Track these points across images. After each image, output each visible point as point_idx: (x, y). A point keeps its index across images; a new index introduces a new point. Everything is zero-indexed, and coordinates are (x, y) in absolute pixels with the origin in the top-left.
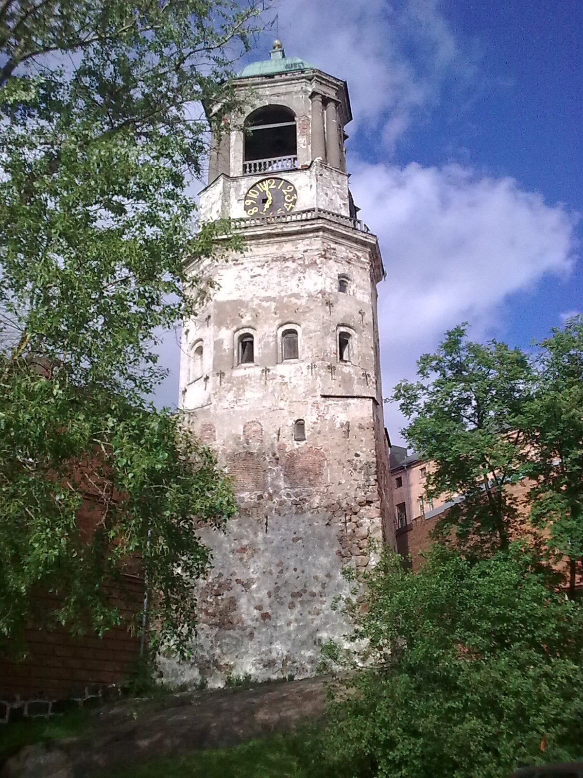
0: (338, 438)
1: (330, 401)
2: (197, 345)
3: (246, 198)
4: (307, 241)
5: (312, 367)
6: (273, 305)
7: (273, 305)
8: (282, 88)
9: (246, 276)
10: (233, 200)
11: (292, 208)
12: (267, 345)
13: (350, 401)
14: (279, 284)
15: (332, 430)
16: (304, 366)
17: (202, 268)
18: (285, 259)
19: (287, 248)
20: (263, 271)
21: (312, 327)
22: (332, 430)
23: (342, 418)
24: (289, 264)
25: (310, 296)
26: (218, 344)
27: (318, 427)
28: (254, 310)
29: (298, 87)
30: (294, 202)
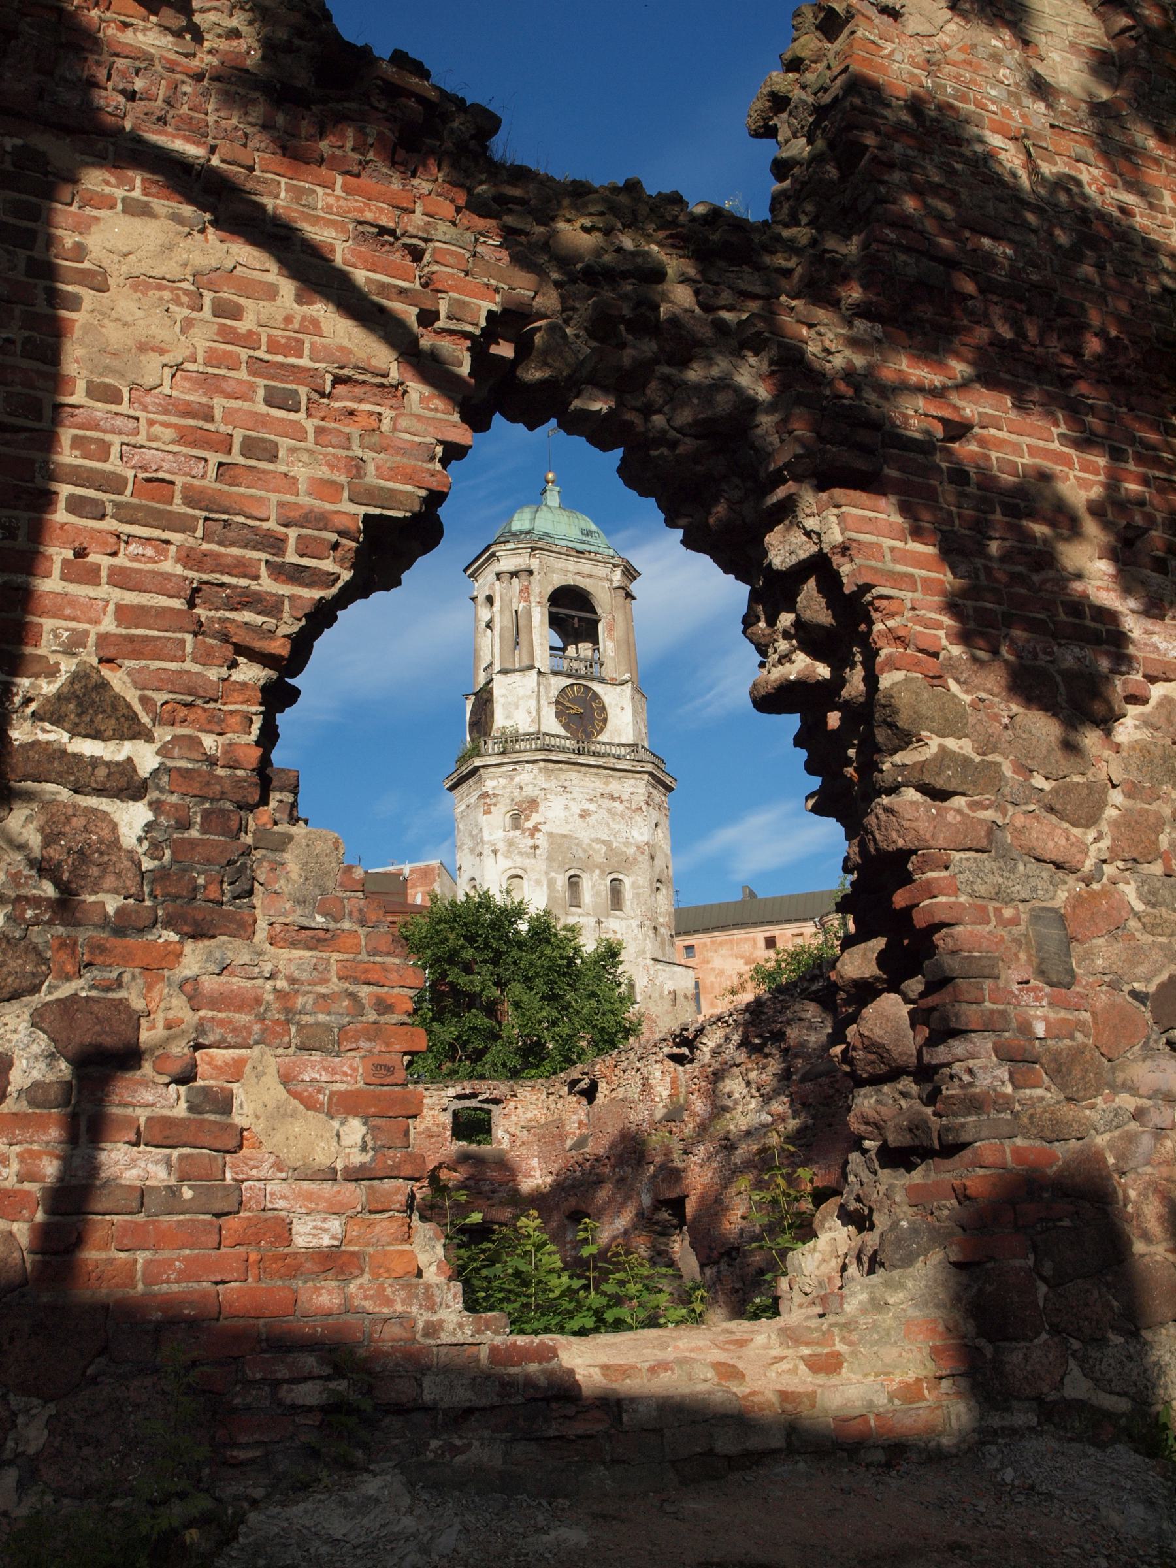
0: (667, 1005)
1: (659, 966)
2: (514, 872)
3: (557, 702)
4: (632, 782)
5: (642, 926)
6: (604, 849)
7: (604, 849)
8: (586, 566)
9: (576, 809)
10: (543, 702)
11: (602, 729)
12: (598, 894)
13: (676, 968)
14: (608, 824)
15: (661, 997)
16: (635, 923)
17: (517, 780)
18: (613, 798)
19: (614, 787)
20: (592, 807)
21: (641, 881)
22: (661, 997)
23: (669, 986)
24: (617, 804)
25: (638, 848)
26: (551, 884)
27: (649, 991)
28: (585, 851)
29: (603, 571)
30: (605, 721)
